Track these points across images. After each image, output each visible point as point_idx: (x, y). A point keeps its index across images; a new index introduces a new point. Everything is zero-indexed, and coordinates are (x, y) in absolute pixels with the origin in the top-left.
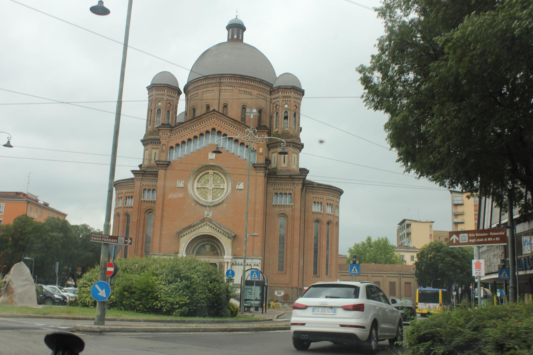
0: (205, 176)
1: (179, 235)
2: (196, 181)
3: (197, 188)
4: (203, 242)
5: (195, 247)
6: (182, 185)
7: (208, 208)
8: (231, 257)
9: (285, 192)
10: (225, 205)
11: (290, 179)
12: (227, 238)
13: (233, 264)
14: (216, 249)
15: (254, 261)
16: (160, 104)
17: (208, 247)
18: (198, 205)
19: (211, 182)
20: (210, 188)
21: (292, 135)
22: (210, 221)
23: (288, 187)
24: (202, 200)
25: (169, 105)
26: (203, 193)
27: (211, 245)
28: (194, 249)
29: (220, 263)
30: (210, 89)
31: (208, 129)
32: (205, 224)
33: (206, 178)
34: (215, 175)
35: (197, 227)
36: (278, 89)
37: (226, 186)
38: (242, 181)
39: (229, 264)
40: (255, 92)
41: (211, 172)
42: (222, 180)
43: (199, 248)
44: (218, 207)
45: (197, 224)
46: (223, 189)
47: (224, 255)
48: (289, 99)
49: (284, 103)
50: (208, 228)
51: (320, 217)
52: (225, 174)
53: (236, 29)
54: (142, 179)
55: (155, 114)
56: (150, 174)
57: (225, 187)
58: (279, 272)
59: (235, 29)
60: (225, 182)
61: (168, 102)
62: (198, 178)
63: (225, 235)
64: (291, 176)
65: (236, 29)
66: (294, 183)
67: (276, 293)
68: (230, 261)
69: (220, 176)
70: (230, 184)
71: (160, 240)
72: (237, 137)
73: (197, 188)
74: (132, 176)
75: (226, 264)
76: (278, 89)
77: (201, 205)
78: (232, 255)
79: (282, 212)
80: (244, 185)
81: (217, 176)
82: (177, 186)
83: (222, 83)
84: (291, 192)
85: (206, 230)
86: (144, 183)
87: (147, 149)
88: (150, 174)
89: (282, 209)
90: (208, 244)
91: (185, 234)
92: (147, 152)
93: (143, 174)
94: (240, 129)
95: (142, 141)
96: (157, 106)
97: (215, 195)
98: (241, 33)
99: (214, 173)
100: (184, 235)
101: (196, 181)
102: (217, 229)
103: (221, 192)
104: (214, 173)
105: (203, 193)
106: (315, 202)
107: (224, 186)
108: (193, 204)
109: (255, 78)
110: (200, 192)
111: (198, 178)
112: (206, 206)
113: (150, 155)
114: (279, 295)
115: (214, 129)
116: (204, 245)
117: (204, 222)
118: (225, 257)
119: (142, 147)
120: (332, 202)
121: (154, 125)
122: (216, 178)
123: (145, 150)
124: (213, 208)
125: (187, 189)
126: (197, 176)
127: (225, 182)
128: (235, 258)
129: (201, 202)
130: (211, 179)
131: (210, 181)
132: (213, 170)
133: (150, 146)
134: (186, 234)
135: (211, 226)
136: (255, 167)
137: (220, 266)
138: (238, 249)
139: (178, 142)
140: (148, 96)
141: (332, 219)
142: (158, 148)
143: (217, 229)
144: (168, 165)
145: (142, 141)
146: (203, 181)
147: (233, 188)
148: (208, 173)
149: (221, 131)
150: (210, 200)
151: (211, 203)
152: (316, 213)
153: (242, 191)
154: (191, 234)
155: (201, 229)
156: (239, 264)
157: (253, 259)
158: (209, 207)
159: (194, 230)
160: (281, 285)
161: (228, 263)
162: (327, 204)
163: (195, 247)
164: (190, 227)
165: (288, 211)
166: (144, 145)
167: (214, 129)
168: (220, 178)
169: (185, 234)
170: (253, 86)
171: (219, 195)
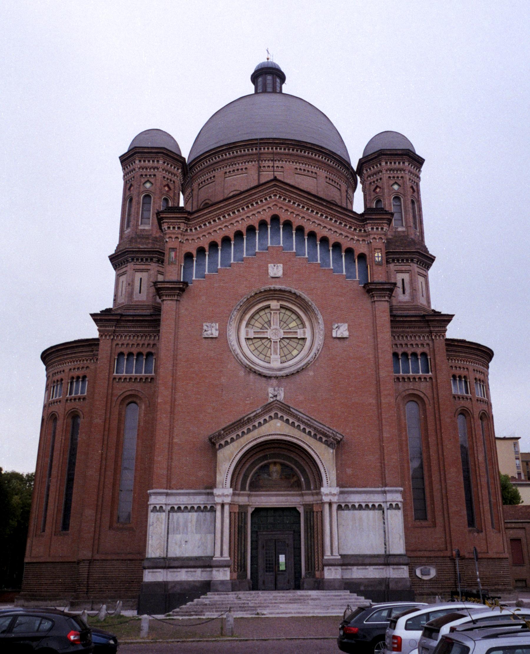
0: (262, 313)
1: (214, 444)
2: (244, 323)
3: (248, 339)
4: (265, 457)
5: (249, 470)
6: (216, 334)
7: (274, 382)
8: (336, 490)
10: (311, 373)
11: (422, 324)
13: (340, 507)
14: (295, 474)
15: (390, 497)
16: (148, 185)
17: (275, 469)
18: (252, 376)
20: (274, 338)
21: (413, 240)
22: (285, 408)
23: (418, 340)
24: (259, 364)
25: (166, 189)
26: (260, 349)
27: (282, 464)
28: (246, 477)
29: (305, 505)
30: (239, 166)
31: (264, 217)
32: (272, 414)
33: (264, 317)
34: (283, 311)
35: (256, 424)
36: (379, 155)
37: (312, 336)
38: (344, 322)
39: (335, 507)
40: (322, 173)
41: (274, 304)
42: (299, 322)
43: (256, 473)
44: (298, 378)
45: (257, 416)
46: (304, 339)
47: (321, 485)
48: (400, 174)
49: (392, 182)
50: (279, 423)
51: (466, 404)
52: (306, 307)
53: (268, 77)
54: (115, 331)
55: (138, 203)
56: (133, 321)
57: (308, 336)
59: (269, 77)
60: (307, 324)
61: (165, 183)
62: (248, 317)
63: (320, 439)
64: (424, 316)
65: (268, 77)
66: (431, 332)
68: (335, 499)
70: (320, 327)
71: (170, 458)
72: (325, 233)
73: (248, 339)
74: (92, 331)
75: (327, 507)
76: (379, 155)
77: (260, 375)
78: (338, 485)
79: (411, 392)
80: (349, 330)
82: (205, 335)
83: (262, 154)
84: (426, 350)
85: (275, 429)
86: (119, 341)
87: (124, 273)
88: (133, 321)
90: (275, 463)
91: (229, 440)
92: (123, 278)
93: (117, 321)
94: (331, 215)
95: (112, 258)
96: (142, 189)
97: (286, 352)
98: (278, 84)
99: (282, 307)
100: (227, 443)
101: (244, 323)
102: (302, 427)
103: (299, 347)
104: (282, 307)
105: (260, 349)
106: (454, 377)
108: (242, 373)
109: (322, 147)
110: (252, 348)
111: (248, 317)
112: (270, 377)
113: (131, 284)
115: (275, 219)
116: (267, 466)
117: (270, 410)
118: (324, 490)
119: (112, 273)
121: (137, 225)
122: (286, 317)
123: (118, 276)
124: (284, 382)
125: (226, 341)
126: (245, 313)
127: (307, 324)
129: (257, 368)
130: (275, 318)
131: (276, 324)
132: (278, 300)
133: (130, 266)
134: (232, 440)
135: (287, 420)
136: (369, 291)
137: (306, 512)
138: (349, 471)
139: (201, 244)
140: (121, 174)
141: (486, 409)
142: (147, 270)
143: (302, 427)
144: (182, 290)
145: (112, 258)
146: (257, 324)
147: (328, 336)
148: (268, 307)
149: (292, 220)
150: (276, 364)
151: (280, 370)
152: (459, 398)
153: (347, 342)
154: (243, 440)
156: (354, 506)
157: (385, 492)
158: (276, 377)
159: (249, 430)
161: (330, 504)
163: (249, 470)
164: (240, 424)
165: (424, 388)
166: (116, 266)
167: (275, 219)
169: (229, 440)
171: (295, 352)
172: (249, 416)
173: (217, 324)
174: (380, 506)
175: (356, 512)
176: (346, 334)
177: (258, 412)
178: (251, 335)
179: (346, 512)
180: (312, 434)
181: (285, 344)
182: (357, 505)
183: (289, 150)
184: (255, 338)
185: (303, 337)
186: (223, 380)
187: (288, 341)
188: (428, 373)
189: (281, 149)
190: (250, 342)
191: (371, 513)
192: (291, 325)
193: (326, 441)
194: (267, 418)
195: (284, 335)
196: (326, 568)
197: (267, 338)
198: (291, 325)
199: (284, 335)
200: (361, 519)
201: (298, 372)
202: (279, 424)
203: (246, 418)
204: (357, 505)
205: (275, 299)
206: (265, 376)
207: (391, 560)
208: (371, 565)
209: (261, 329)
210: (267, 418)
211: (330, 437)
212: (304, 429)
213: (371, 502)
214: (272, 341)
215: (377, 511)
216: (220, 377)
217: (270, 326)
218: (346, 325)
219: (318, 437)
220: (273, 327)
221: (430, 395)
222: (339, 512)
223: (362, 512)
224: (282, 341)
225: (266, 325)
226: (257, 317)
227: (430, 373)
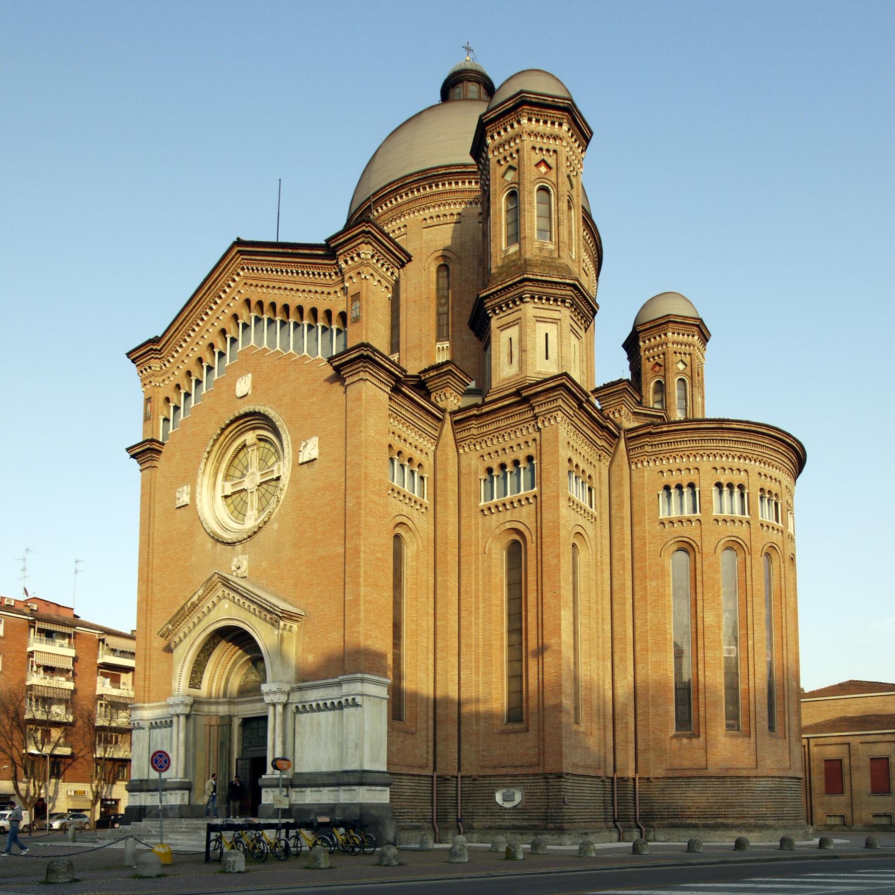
2: (220, 476)
9: (513, 456)
12: (269, 626)
19: (254, 468)
32: (220, 594)
35: (205, 610)
58: (510, 727)
67: (499, 798)
68: (276, 698)
73: (226, 497)
89: (508, 516)
101: (220, 476)
114: (508, 805)
128: (300, 689)
155: (214, 615)
160: (511, 771)
172: (192, 601)
174: (340, 702)
175: (314, 714)
177: (200, 593)
179: (305, 715)
180: (257, 612)
182: (314, 704)
187: (265, 486)
188: (533, 487)
190: (229, 500)
191: (331, 713)
192: (269, 464)
194: (215, 599)
196: (263, 790)
197: (244, 490)
198: (269, 464)
201: (260, 528)
202: (226, 606)
203: (189, 604)
204: (314, 704)
206: (229, 544)
207: (369, 779)
208: (324, 785)
210: (215, 599)
215: (337, 711)
219: (262, 616)
220: (250, 471)
221: (532, 526)
223: (322, 713)
225: (245, 472)
226: (237, 461)
227: (535, 489)
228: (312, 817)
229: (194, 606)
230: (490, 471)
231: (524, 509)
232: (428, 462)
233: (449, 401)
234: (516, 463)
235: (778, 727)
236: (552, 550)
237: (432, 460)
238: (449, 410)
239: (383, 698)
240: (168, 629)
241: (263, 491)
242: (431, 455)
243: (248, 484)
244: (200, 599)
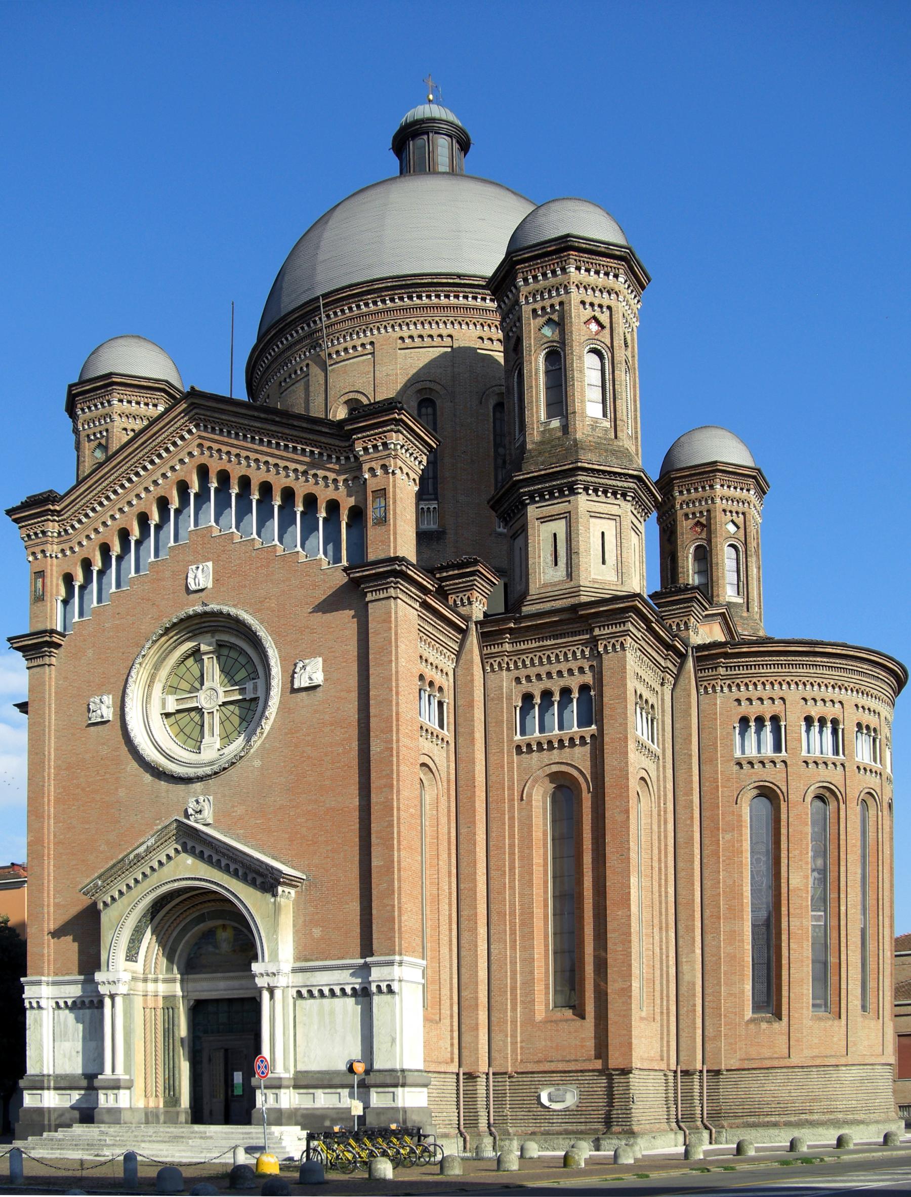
7: (198, 786)
9: (562, 683)
34: (225, 652)
50: (190, 860)
69: (242, 652)
73: (167, 715)
81: (233, 654)
107: (255, 689)
120: (831, 712)
135: (202, 852)
143: (224, 862)
151: (211, 763)
158: (200, 779)
162: (809, 720)
168: (242, 660)
170: (455, 307)
173: (111, 696)
176: (319, 678)
178: (171, 707)
180: (240, 874)
181: (228, 713)
183: (384, 302)
184: (178, 711)
185: (253, 696)
186: (122, 793)
189: (367, 305)
193: (263, 882)
195: (225, 697)
199: (225, 697)
200: (332, 1013)
205: (207, 632)
209: (190, 692)
211: (266, 875)
212: (228, 865)
213: (348, 984)
214: (206, 711)
216: (117, 789)
217: (202, 684)
218: (320, 660)
220: (207, 684)
222: (299, 1002)
224: (222, 708)
227: (594, 727)
228: (327, 1123)
229: (139, 858)
230: (528, 698)
231: (577, 750)
232: (447, 683)
233: (474, 606)
234: (566, 692)
235: (872, 1006)
236: (618, 803)
237: (452, 680)
238: (474, 619)
239: (419, 983)
240: (96, 885)
241: (228, 713)
242: (451, 674)
243: (203, 700)
244: (148, 851)
